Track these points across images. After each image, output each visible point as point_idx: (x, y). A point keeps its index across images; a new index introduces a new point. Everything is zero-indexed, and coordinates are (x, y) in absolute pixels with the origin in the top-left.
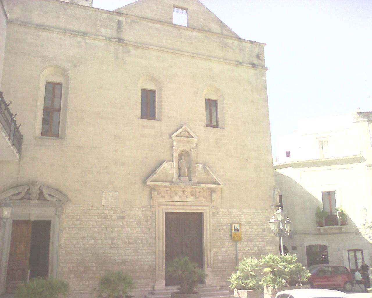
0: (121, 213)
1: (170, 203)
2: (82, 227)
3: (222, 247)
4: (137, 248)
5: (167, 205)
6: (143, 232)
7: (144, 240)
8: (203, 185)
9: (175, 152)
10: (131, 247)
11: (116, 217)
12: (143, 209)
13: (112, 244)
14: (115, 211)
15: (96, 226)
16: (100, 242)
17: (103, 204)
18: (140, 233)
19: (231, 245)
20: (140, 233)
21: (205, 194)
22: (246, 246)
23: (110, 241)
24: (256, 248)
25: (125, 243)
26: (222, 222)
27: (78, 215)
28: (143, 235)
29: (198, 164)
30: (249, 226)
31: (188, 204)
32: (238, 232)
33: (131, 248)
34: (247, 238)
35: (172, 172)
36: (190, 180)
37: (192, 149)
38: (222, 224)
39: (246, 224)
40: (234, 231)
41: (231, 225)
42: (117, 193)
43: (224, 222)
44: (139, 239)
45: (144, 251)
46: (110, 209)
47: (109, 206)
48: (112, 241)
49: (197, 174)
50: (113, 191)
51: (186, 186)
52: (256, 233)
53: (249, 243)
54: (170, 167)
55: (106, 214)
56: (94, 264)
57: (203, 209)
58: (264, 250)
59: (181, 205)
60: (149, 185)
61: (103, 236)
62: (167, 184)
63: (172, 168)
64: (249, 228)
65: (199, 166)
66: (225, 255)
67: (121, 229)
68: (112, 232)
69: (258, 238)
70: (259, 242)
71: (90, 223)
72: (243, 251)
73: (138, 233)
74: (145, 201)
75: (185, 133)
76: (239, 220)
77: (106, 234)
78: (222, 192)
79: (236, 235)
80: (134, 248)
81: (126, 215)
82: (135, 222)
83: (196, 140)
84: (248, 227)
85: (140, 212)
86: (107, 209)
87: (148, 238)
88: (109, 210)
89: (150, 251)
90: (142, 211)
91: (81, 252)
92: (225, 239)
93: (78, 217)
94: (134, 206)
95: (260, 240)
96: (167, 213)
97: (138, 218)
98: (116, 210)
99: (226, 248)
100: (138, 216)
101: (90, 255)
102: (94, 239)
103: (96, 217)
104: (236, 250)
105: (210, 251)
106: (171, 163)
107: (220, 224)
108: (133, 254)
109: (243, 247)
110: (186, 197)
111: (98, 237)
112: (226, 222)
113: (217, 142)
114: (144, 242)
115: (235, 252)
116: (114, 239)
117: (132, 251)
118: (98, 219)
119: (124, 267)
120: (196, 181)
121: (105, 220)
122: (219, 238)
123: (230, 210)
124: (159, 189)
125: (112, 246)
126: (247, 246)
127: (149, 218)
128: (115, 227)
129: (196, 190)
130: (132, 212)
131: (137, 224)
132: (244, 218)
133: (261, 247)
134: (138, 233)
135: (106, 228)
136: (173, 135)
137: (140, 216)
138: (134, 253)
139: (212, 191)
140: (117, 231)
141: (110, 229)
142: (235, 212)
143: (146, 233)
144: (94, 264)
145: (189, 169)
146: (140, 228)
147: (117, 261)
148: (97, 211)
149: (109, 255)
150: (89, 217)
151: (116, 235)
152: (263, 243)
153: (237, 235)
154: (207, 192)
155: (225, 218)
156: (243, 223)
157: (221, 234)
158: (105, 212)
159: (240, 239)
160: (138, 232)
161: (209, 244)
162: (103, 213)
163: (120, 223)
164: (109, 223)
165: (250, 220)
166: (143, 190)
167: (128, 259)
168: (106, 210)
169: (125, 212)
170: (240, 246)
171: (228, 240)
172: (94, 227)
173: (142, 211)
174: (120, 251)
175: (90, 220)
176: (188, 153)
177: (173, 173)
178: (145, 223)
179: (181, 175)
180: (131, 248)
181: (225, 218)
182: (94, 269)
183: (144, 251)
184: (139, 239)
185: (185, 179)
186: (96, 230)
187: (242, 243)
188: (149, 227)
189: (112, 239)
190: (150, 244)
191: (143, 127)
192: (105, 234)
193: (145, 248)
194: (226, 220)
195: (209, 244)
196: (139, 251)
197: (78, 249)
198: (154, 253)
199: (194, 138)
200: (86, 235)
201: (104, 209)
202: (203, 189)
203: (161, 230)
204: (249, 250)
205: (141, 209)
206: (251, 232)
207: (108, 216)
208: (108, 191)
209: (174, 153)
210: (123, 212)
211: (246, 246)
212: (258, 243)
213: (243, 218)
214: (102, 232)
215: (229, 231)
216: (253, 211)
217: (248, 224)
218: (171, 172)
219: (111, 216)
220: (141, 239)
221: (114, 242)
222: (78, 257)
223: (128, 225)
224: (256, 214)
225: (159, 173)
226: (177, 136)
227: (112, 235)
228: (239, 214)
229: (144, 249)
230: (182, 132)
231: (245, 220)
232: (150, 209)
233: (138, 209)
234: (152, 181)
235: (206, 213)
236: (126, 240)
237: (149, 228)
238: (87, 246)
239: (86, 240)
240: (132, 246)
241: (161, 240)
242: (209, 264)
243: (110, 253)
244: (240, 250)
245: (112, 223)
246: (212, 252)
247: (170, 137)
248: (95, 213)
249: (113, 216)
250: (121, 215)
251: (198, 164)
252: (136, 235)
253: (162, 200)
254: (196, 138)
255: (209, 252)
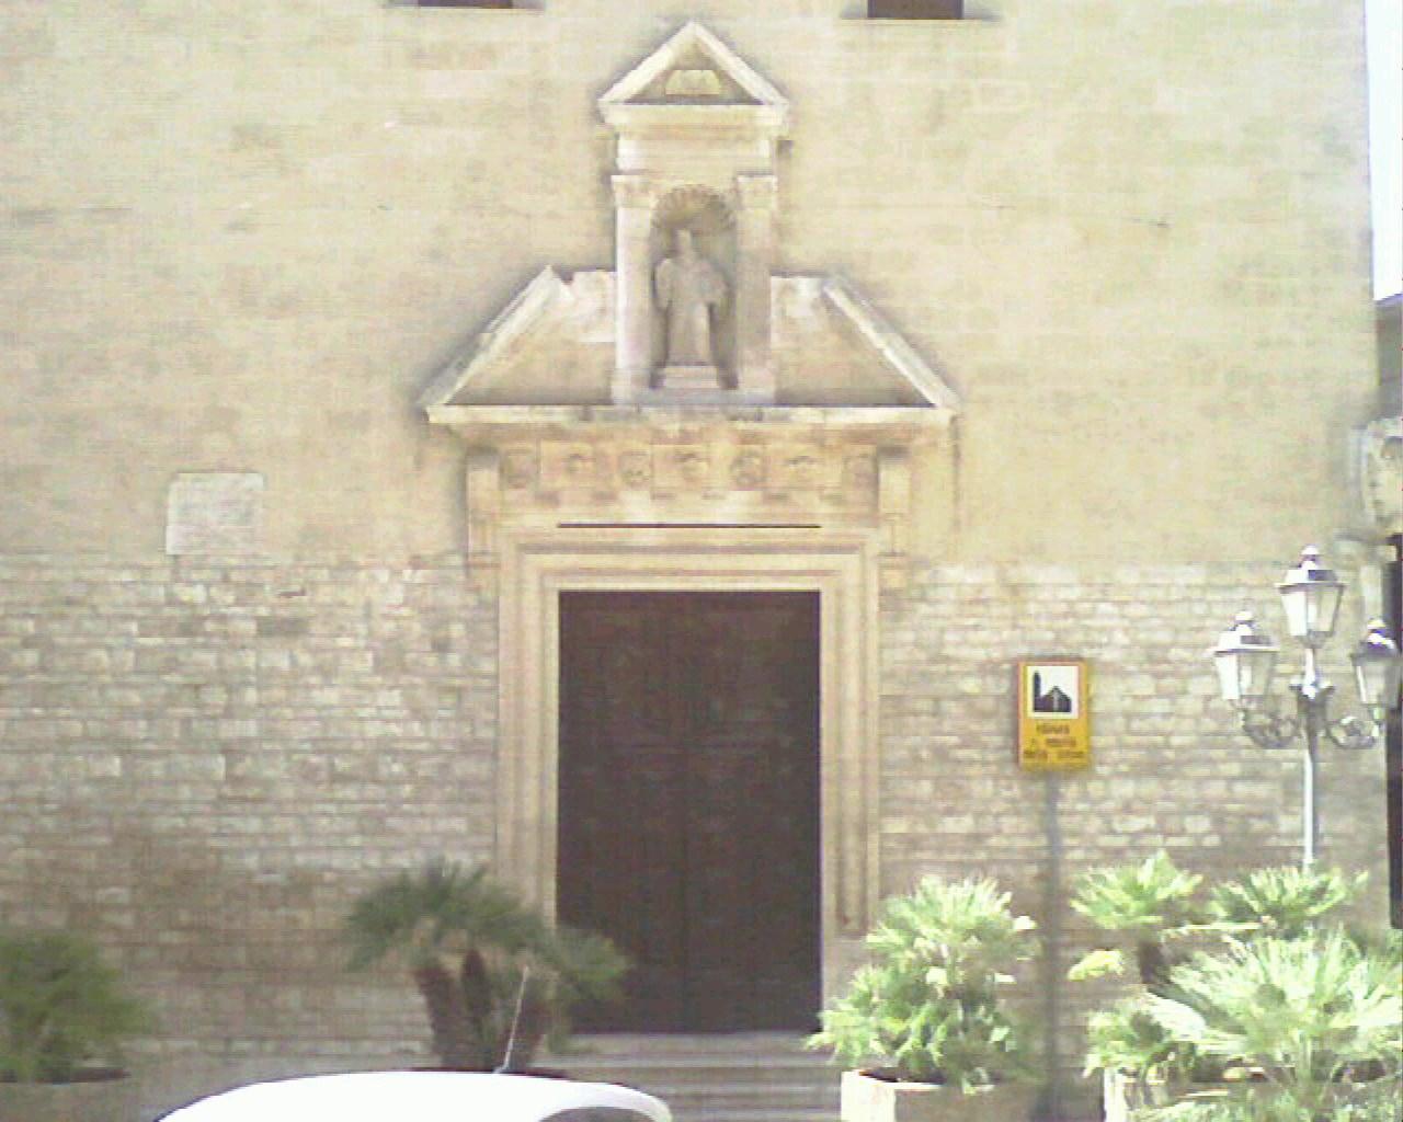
0: (284, 600)
1: (610, 536)
2: (56, 680)
3: (949, 812)
4: (382, 806)
5: (565, 548)
6: (418, 713)
7: (424, 762)
8: (806, 416)
9: (629, 205)
10: (341, 802)
11: (251, 627)
12: (420, 576)
13: (232, 779)
14: (247, 593)
15: (134, 679)
16: (157, 768)
17: (170, 550)
18: (397, 721)
19: (1013, 801)
20: (397, 721)
21: (830, 474)
22: (1127, 809)
23: (219, 765)
24: (1198, 824)
25: (309, 774)
26: (950, 651)
27: (27, 616)
28: (416, 728)
29: (793, 274)
30: (1158, 676)
31: (720, 543)
32: (1062, 715)
33: (346, 808)
34: (1133, 755)
35: (608, 339)
36: (730, 382)
37: (741, 179)
38: (953, 668)
39: (1132, 668)
40: (1036, 709)
41: (1015, 675)
42: (254, 481)
43: (965, 652)
44: (395, 753)
45: (425, 825)
46: (218, 576)
47: (211, 561)
48: (229, 766)
49: (775, 341)
50: (233, 470)
51: (692, 426)
52: (1209, 724)
53: (1151, 787)
54: (590, 303)
55: (192, 605)
56: (123, 895)
57: (825, 573)
58: (1266, 835)
59: (727, 550)
60: (447, 429)
61: (176, 735)
62: (560, 415)
63: (603, 311)
64: (1158, 689)
65: (792, 289)
66: (965, 857)
67: (278, 694)
68: (229, 713)
69: (1220, 753)
70: (1232, 780)
71: (98, 661)
72: (1106, 841)
73: (387, 721)
74: (432, 530)
75: (695, 74)
76: (1079, 637)
77: (195, 725)
78: (957, 454)
79: (1052, 736)
80: (360, 807)
81: (312, 611)
82: (369, 656)
83: (770, 118)
84: (1144, 685)
85: (397, 595)
86: (195, 576)
87: (449, 747)
88: (208, 585)
89: (459, 825)
90: (409, 587)
91: (49, 823)
92: (971, 762)
93: (30, 626)
94: (361, 560)
95: (1234, 769)
96: (569, 601)
97: (388, 627)
98: (249, 584)
99: (979, 815)
100: (386, 617)
101: (103, 840)
102: (126, 749)
103: (134, 627)
104: (1053, 834)
105: (863, 833)
106: (599, 281)
107: (942, 668)
108: (356, 841)
109: (1106, 816)
110: (698, 497)
111: (146, 740)
112: (980, 654)
113: (937, 118)
114: (421, 773)
115: (1043, 841)
116: (244, 753)
117: (351, 824)
118: (142, 635)
119: (304, 917)
120: (768, 390)
121: (180, 641)
122: (924, 754)
123: (1014, 575)
124: (524, 452)
125: (228, 791)
126: (1137, 806)
127: (457, 630)
128: (247, 684)
129: (772, 446)
130: (348, 595)
131: (380, 667)
132: (1115, 622)
133: (1246, 816)
134: (387, 721)
135: (197, 687)
136: (607, 97)
137: (396, 619)
138: (362, 832)
139: (891, 448)
140: (260, 705)
141: (216, 697)
142: (1054, 583)
143: (440, 719)
144: (123, 895)
145: (720, 319)
146: (396, 693)
147: (262, 879)
148: (141, 588)
149: (213, 843)
150: (88, 625)
151: (251, 728)
152: (1262, 790)
153: (1060, 736)
154: (846, 461)
155: (976, 628)
156: (1108, 655)
157: (947, 726)
158: (185, 598)
159: (1079, 764)
160: (386, 713)
161: (852, 794)
162: (172, 601)
163: (278, 658)
164: (208, 658)
165: (1163, 637)
166: (420, 462)
167: (330, 869)
168: (191, 583)
169: (303, 593)
170: (1080, 807)
171: (993, 768)
172: (122, 685)
173: (409, 587)
174: (279, 824)
175: (99, 646)
176: (723, 206)
177: (613, 345)
178: (432, 660)
179: (673, 358)
180: (346, 808)
181: (976, 628)
182: (127, 920)
183: (425, 825)
184: (395, 753)
185: (701, 379)
186: (135, 698)
187: (1095, 788)
188: (457, 682)
189: (229, 751)
190: (463, 783)
191: (418, 57)
192: (187, 721)
193: (430, 808)
194: (989, 640)
195: (852, 794)
196: (392, 822)
197: (33, 808)
198: (488, 840)
199: (758, 102)
200: (76, 728)
201: (177, 580)
202: (817, 437)
203: (532, 702)
204: (1147, 831)
205: (407, 573)
206: (1166, 716)
207: (205, 618)
208: (203, 471)
209: (621, 213)
210: (295, 594)
211: (1127, 809)
212: (1216, 789)
213: (1107, 623)
214: (171, 711)
215: (1005, 709)
216: (1197, 576)
217: (1146, 666)
218: (596, 337)
219: (223, 619)
220: (409, 752)
221: (239, 770)
222: (37, 854)
223: (327, 673)
224: (1210, 596)
225: (515, 346)
226: (640, 99)
227: (229, 730)
228: (1082, 600)
229: (423, 815)
230: (675, 67)
231: (1120, 638)
232: (462, 578)
233: (384, 576)
234: (465, 400)
235: (839, 594)
236: (314, 759)
237: (459, 692)
238: (85, 791)
239: (79, 758)
240: (350, 792)
241: (532, 766)
242: (852, 912)
243: (217, 835)
244: (1074, 834)
245: (231, 661)
246: (873, 844)
247: (597, 116)
248: (127, 604)
249: (233, 617)
250: (283, 613)
251: (784, 274)
252: (373, 730)
253: (538, 521)
254: (771, 104)
255: (851, 841)
